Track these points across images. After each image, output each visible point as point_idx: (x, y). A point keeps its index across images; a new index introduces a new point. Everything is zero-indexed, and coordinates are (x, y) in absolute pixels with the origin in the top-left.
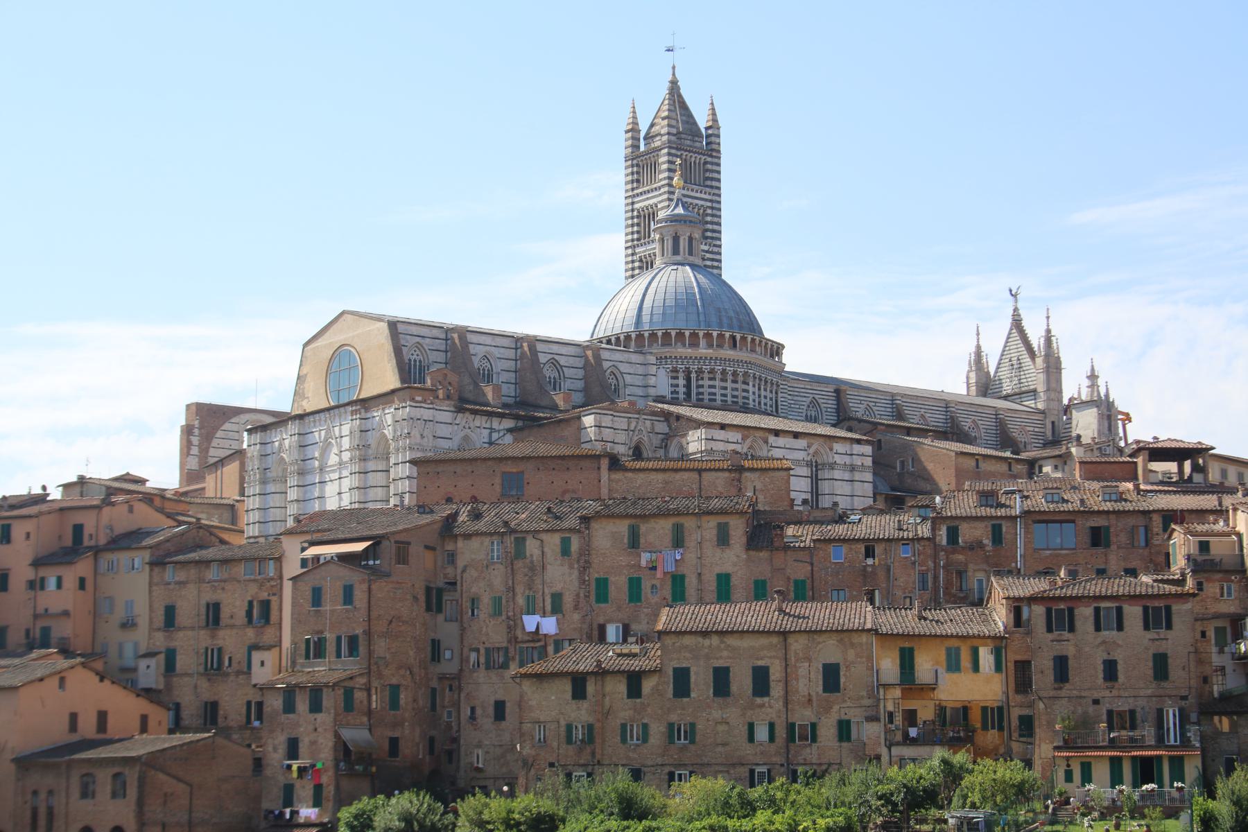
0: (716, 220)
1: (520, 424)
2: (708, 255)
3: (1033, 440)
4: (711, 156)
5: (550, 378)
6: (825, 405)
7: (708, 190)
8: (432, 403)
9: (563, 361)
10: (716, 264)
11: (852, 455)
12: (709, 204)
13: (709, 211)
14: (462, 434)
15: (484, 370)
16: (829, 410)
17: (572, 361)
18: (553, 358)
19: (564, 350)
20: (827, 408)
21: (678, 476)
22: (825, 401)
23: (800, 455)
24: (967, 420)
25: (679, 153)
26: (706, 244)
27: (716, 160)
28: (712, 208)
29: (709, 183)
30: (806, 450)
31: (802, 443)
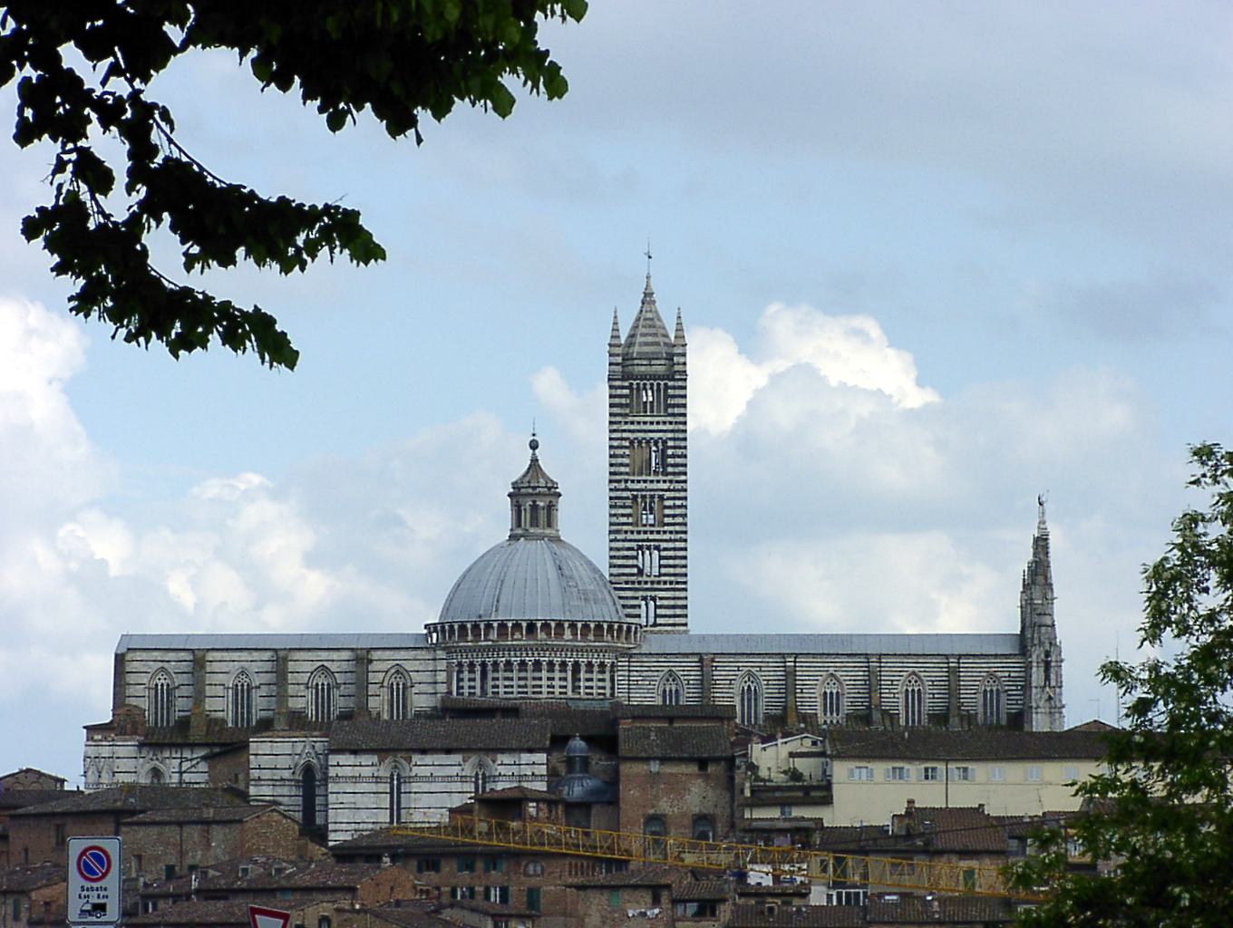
0: (679, 452)
1: (217, 750)
2: (668, 494)
3: (1007, 688)
4: (674, 380)
5: (323, 684)
6: (686, 678)
7: (669, 419)
8: (113, 740)
9: (333, 667)
10: (678, 503)
11: (520, 765)
12: (670, 435)
13: (670, 443)
14: (148, 766)
15: (242, 685)
16: (691, 682)
17: (345, 666)
18: (323, 665)
19: (335, 655)
20: (688, 680)
21: (167, 828)
22: (686, 673)
23: (454, 771)
24: (901, 674)
25: (626, 384)
26: (665, 482)
27: (680, 383)
28: (674, 439)
29: (670, 411)
30: (460, 765)
31: (457, 758)
